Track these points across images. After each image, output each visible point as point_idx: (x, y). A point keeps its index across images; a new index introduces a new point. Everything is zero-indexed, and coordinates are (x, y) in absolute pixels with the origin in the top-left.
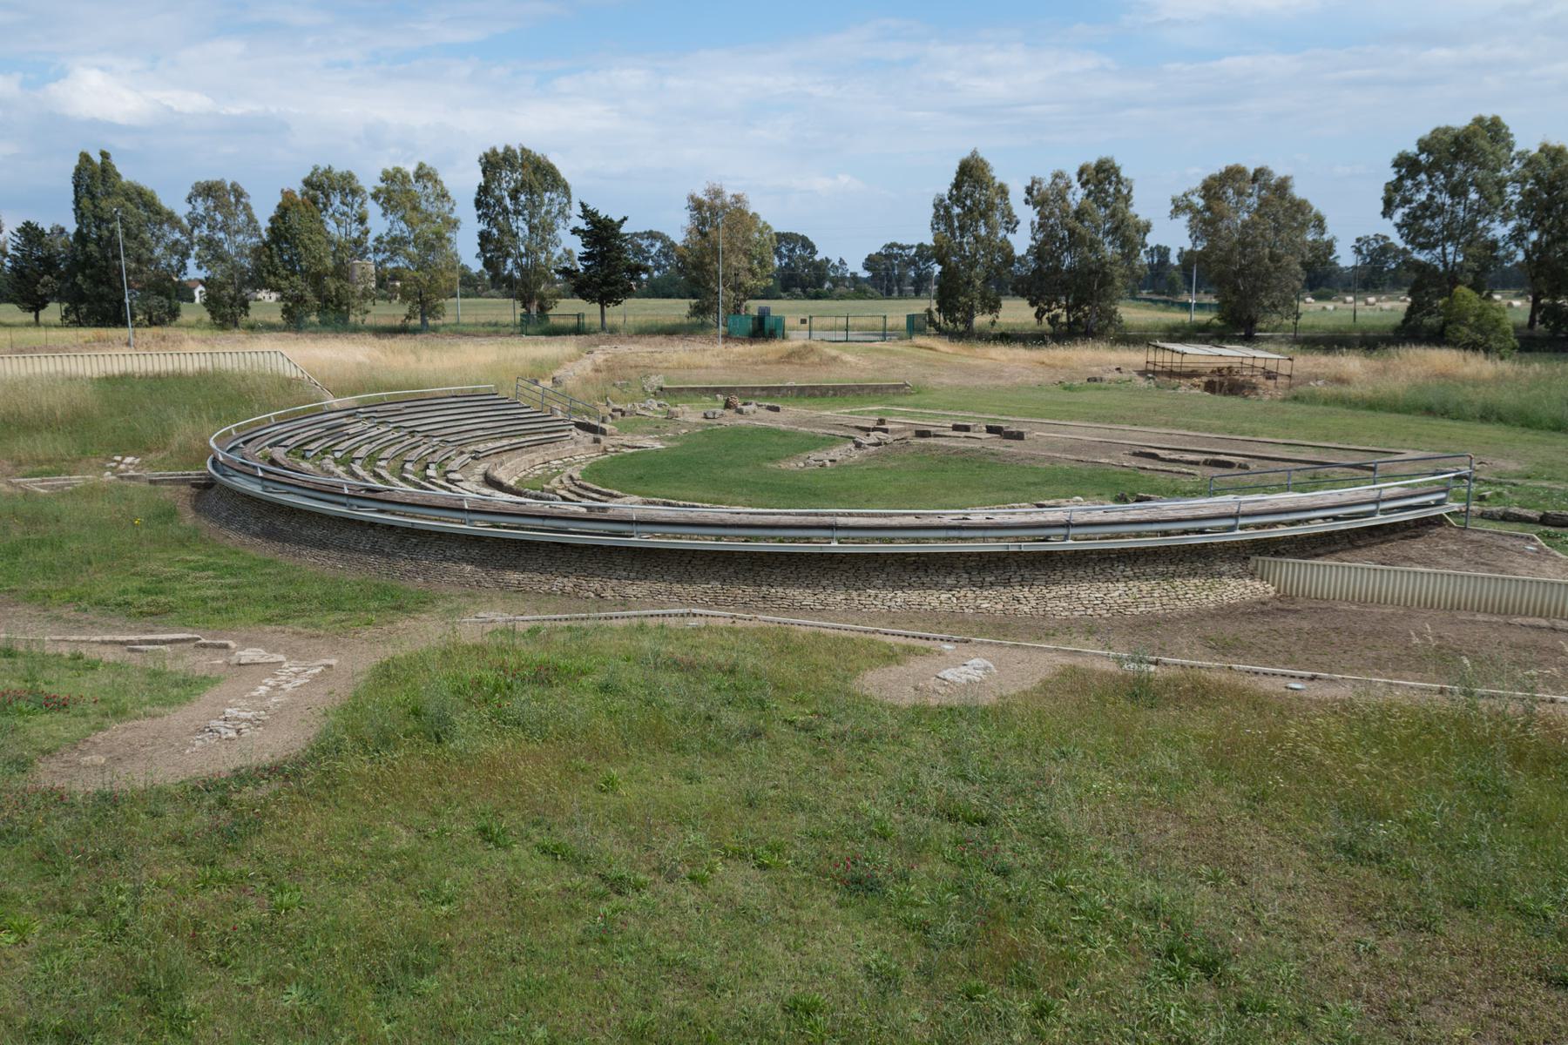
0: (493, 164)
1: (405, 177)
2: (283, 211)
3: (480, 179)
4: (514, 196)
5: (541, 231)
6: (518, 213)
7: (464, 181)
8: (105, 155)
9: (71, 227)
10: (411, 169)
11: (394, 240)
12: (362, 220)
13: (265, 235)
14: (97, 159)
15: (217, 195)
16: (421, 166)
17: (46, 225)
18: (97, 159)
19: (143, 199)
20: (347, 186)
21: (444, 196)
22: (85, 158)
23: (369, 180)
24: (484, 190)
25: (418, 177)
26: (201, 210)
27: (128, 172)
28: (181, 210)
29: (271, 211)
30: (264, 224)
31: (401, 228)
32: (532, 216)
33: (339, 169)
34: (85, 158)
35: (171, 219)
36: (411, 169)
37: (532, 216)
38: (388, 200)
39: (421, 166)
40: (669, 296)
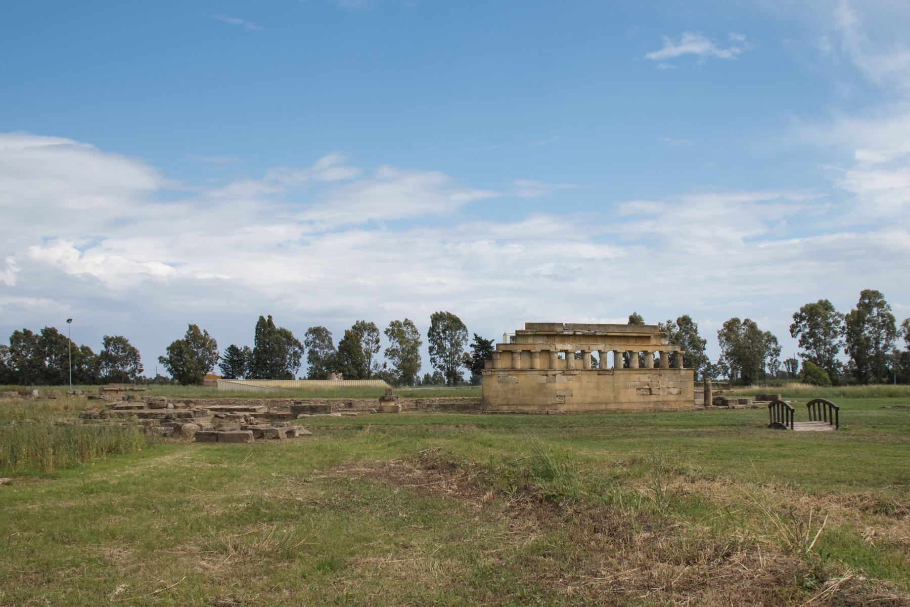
0: (437, 318)
1: (400, 325)
2: (348, 336)
3: (431, 325)
4: (444, 332)
5: (456, 345)
6: (445, 338)
7: (423, 324)
8: (270, 317)
9: (252, 346)
10: (402, 321)
11: (393, 350)
12: (377, 341)
13: (337, 349)
14: (266, 319)
15: (318, 333)
16: (406, 320)
17: (240, 346)
18: (266, 319)
19: (287, 336)
20: (372, 328)
21: (416, 332)
22: (262, 318)
23: (383, 324)
24: (432, 329)
25: (405, 324)
26: (310, 339)
27: (278, 324)
28: (302, 340)
29: (342, 337)
30: (336, 344)
31: (397, 345)
32: (451, 340)
33: (367, 321)
34: (262, 318)
35: (297, 343)
36: (402, 321)
37: (451, 340)
38: (392, 334)
39: (406, 320)
40: (598, 325)
